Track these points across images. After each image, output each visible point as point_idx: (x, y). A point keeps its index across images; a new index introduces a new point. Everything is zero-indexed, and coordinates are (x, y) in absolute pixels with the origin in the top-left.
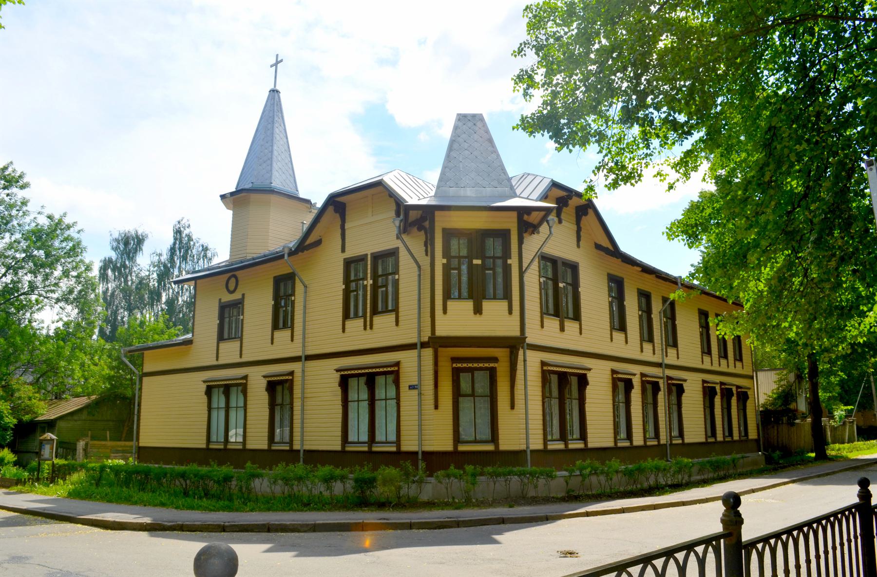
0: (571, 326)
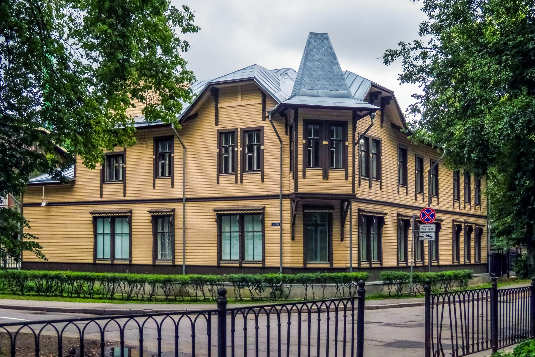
0: (376, 185)
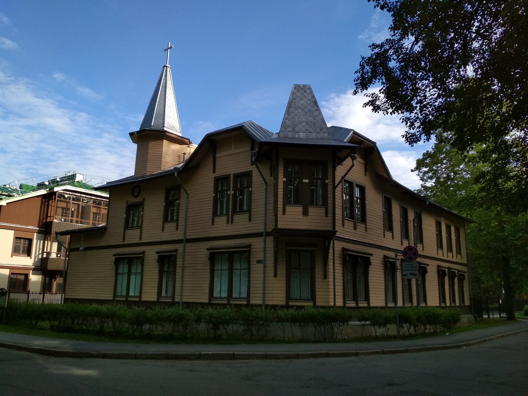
0: (361, 227)
